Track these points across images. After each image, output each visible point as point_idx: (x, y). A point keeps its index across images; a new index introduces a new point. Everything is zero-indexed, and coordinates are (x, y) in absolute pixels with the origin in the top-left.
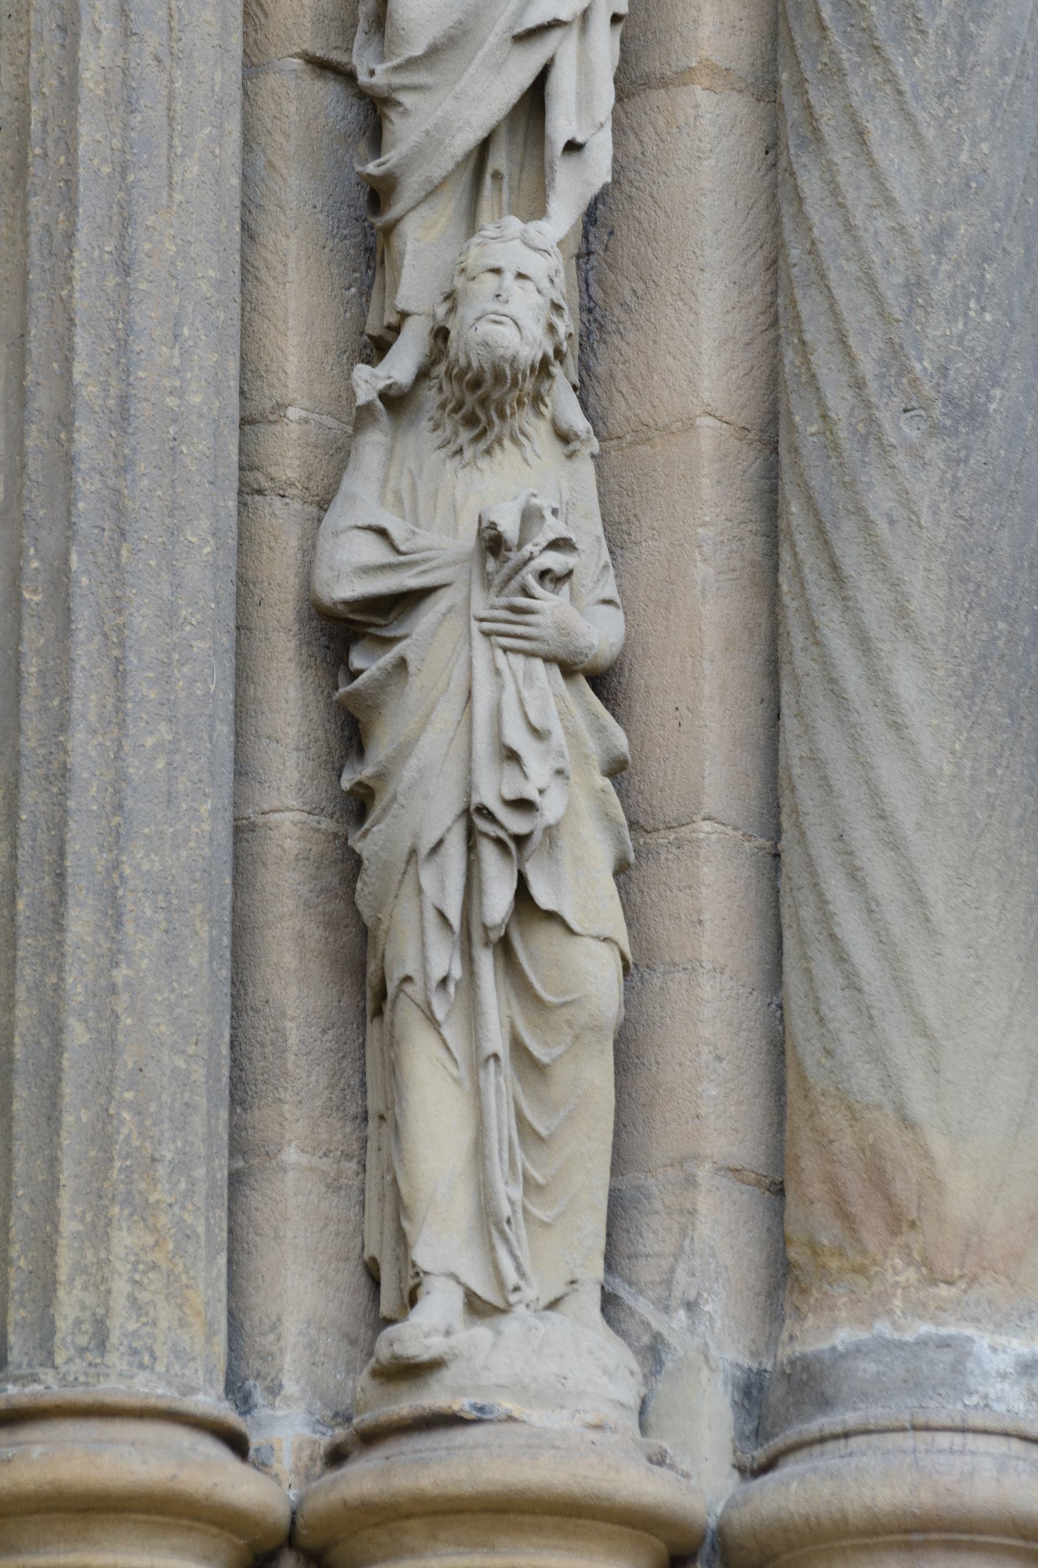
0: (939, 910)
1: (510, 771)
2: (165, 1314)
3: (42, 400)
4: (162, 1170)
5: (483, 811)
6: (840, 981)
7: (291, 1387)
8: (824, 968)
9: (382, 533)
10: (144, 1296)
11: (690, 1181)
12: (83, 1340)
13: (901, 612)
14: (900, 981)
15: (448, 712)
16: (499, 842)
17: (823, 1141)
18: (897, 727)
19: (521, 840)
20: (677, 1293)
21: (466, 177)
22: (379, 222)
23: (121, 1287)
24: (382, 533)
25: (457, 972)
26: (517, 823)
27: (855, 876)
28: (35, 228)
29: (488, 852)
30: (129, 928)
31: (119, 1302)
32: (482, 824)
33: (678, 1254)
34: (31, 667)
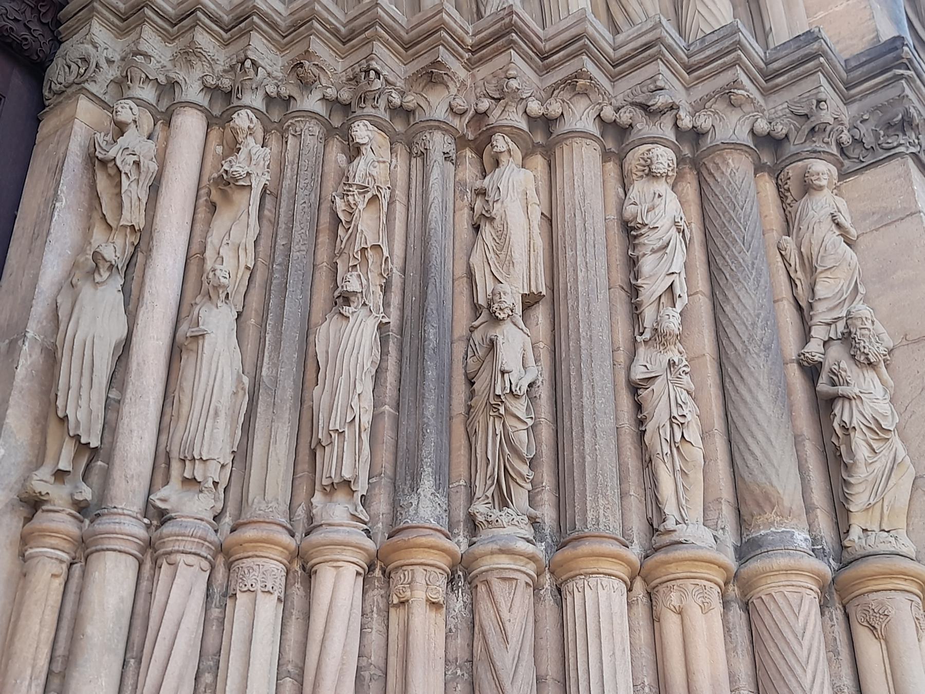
0: (774, 443)
1: (680, 409)
2: (611, 518)
3: (573, 337)
4: (609, 488)
5: (674, 417)
6: (752, 459)
7: (636, 541)
8: (747, 456)
9: (646, 366)
10: (606, 514)
11: (721, 502)
12: (594, 523)
13: (758, 384)
14: (767, 457)
15: (665, 397)
16: (678, 424)
17: (752, 493)
18: (760, 407)
19: (682, 424)
20: (719, 527)
21: (656, 302)
22: (638, 312)
23: (601, 512)
24: (646, 366)
25: (669, 452)
26: (681, 420)
27: (753, 437)
28: (570, 306)
29: (675, 426)
30: (598, 438)
31: (601, 515)
32: (674, 420)
33: (718, 518)
34: (573, 387)
